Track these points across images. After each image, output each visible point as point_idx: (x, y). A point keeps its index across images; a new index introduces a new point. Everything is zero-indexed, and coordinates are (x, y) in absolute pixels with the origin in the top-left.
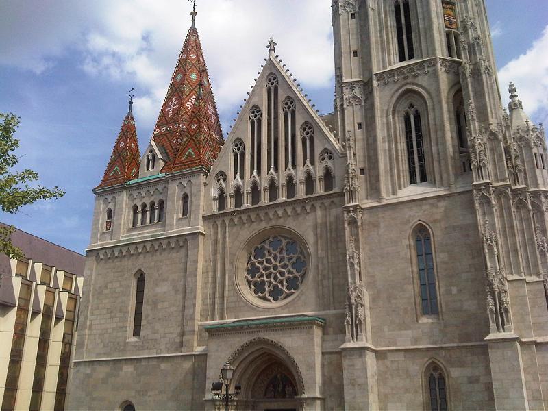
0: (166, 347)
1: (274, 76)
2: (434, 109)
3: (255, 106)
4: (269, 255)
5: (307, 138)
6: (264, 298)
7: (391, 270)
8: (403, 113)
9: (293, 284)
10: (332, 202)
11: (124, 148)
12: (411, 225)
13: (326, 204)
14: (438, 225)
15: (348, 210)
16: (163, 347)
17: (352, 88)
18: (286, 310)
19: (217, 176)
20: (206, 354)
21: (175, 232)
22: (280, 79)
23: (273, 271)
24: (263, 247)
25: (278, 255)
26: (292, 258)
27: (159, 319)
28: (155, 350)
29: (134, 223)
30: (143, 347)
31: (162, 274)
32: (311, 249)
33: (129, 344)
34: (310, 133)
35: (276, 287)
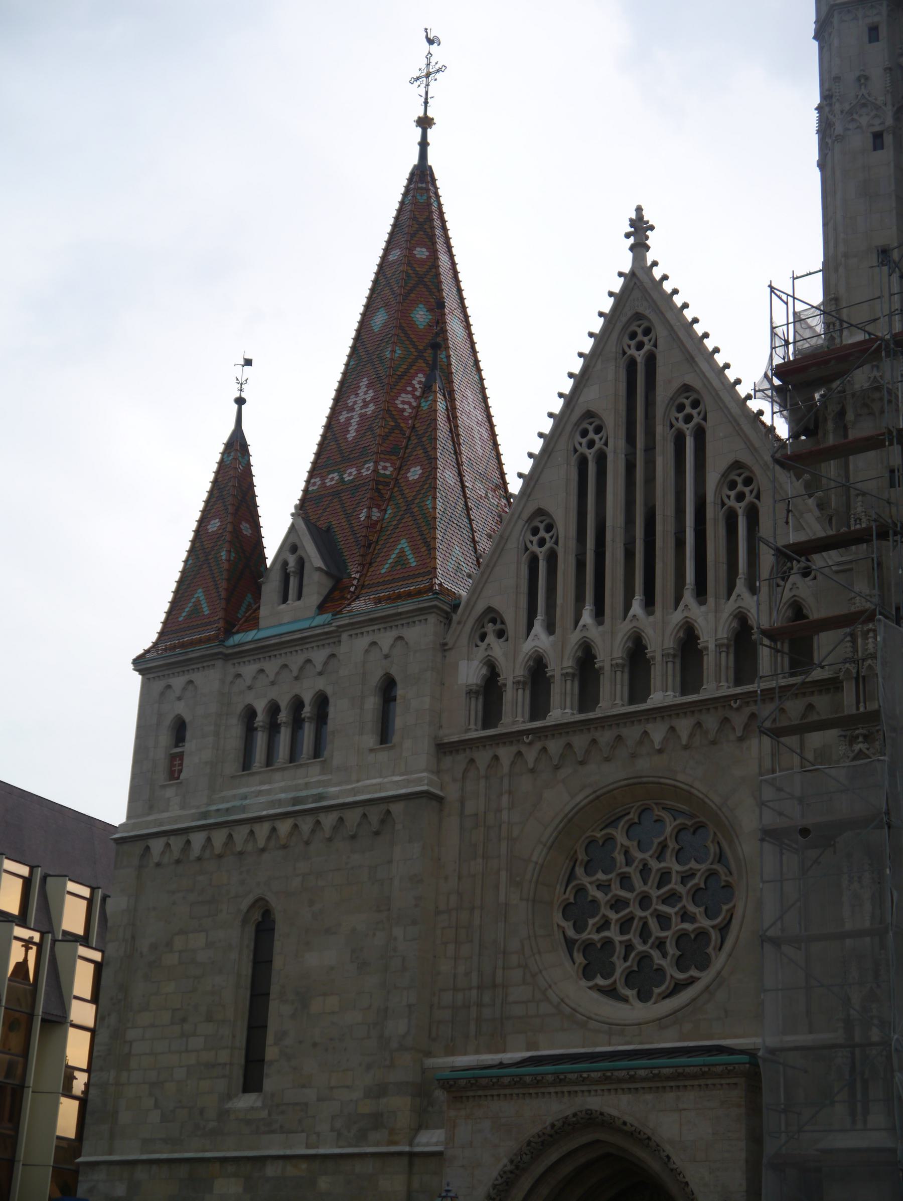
0: (332, 1130)
3: (589, 415)
4: (629, 862)
5: (740, 512)
6: (611, 992)
19: (480, 622)
22: (660, 331)
23: (639, 913)
24: (610, 839)
25: (654, 865)
26: (693, 875)
27: (315, 1045)
28: (304, 1135)
29: (246, 764)
34: (749, 498)
35: (644, 958)
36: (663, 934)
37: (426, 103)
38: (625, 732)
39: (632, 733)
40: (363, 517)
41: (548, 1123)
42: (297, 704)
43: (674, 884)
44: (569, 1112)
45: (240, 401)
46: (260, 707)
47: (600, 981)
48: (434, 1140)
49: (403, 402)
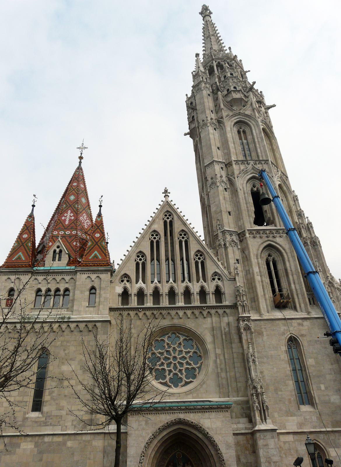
0: (72, 425)
1: (169, 214)
2: (289, 261)
3: (155, 231)
7: (275, 369)
8: (265, 258)
9: (192, 374)
10: (225, 312)
11: (27, 240)
12: (286, 336)
13: (220, 313)
14: (305, 338)
15: (244, 319)
16: (69, 424)
17: (231, 235)
18: (191, 395)
20: (127, 432)
21: (84, 318)
27: (65, 396)
28: (60, 427)
30: (46, 423)
31: (68, 353)
32: (209, 346)
33: (29, 420)
36: (181, 368)
37: (81, 154)
38: (171, 312)
39: (173, 312)
40: (75, 244)
41: (166, 422)
42: (58, 290)
43: (184, 354)
44: (173, 419)
45: (33, 206)
46: (44, 289)
47: (161, 380)
48: (113, 428)
49: (82, 219)
